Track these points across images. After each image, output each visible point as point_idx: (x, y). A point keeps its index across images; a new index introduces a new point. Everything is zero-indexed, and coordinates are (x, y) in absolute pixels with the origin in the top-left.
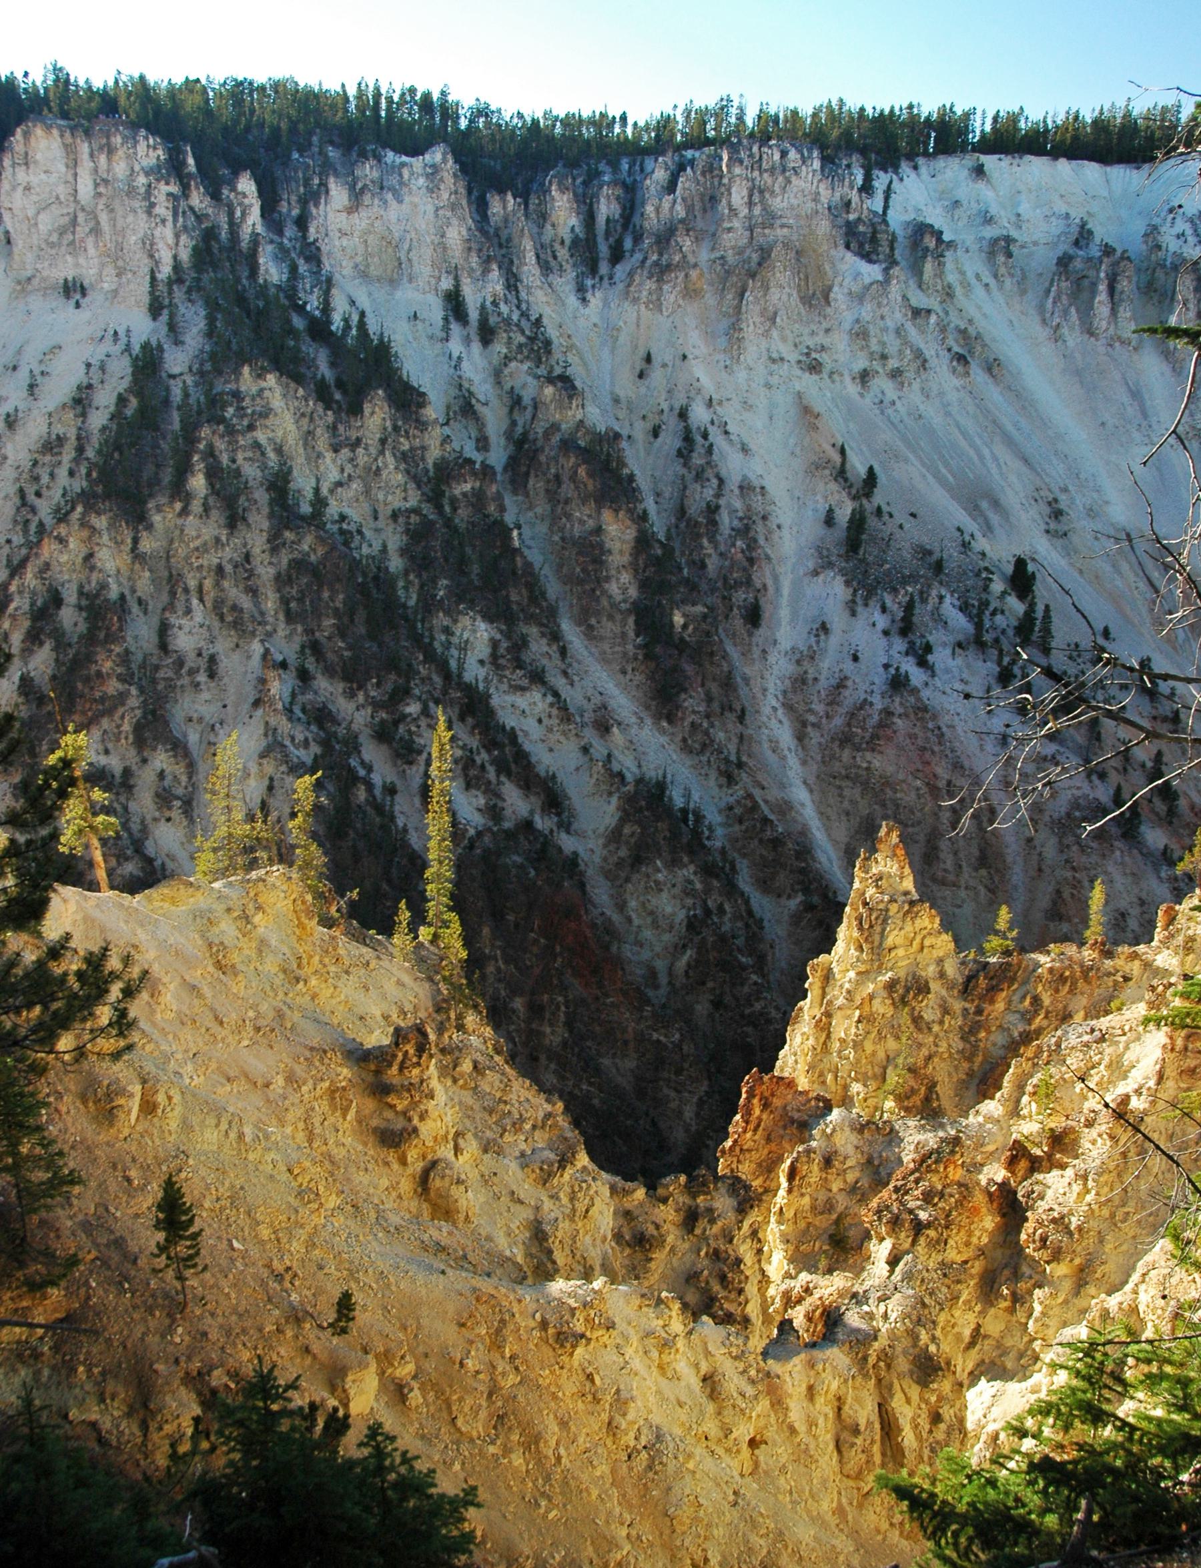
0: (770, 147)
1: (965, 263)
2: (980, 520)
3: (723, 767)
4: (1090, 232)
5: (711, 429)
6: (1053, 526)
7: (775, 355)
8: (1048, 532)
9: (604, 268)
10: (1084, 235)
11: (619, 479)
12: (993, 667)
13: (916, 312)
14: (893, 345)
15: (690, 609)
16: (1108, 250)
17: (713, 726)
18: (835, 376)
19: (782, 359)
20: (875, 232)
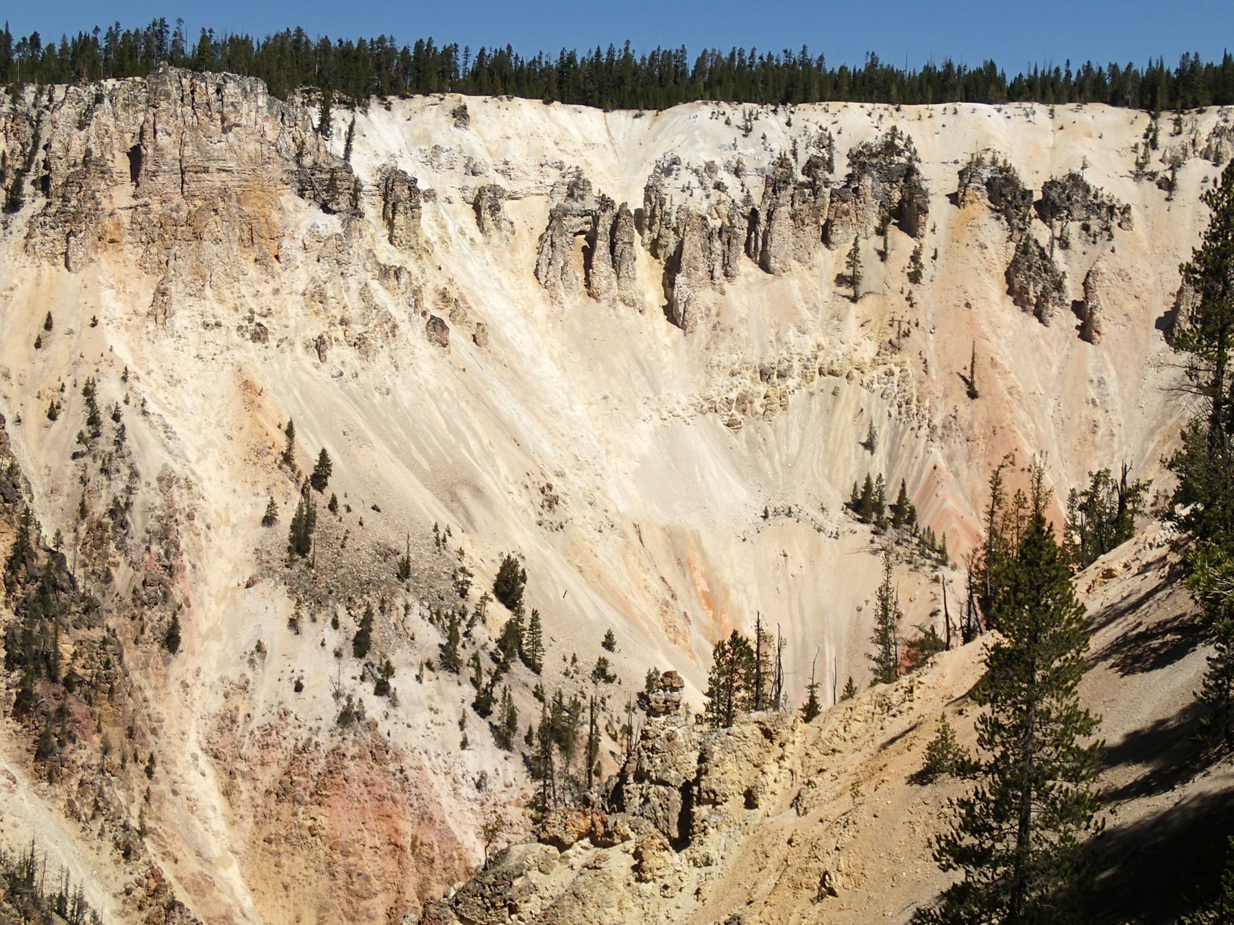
0: (204, 79)
1: (445, 219)
2: (460, 510)
3: (120, 836)
5: (124, 409)
6: (547, 516)
10: (576, 188)
12: (470, 693)
15: (83, 633)
16: (605, 203)
17: (109, 784)
18: (284, 345)
19: (218, 325)
20: (333, 180)
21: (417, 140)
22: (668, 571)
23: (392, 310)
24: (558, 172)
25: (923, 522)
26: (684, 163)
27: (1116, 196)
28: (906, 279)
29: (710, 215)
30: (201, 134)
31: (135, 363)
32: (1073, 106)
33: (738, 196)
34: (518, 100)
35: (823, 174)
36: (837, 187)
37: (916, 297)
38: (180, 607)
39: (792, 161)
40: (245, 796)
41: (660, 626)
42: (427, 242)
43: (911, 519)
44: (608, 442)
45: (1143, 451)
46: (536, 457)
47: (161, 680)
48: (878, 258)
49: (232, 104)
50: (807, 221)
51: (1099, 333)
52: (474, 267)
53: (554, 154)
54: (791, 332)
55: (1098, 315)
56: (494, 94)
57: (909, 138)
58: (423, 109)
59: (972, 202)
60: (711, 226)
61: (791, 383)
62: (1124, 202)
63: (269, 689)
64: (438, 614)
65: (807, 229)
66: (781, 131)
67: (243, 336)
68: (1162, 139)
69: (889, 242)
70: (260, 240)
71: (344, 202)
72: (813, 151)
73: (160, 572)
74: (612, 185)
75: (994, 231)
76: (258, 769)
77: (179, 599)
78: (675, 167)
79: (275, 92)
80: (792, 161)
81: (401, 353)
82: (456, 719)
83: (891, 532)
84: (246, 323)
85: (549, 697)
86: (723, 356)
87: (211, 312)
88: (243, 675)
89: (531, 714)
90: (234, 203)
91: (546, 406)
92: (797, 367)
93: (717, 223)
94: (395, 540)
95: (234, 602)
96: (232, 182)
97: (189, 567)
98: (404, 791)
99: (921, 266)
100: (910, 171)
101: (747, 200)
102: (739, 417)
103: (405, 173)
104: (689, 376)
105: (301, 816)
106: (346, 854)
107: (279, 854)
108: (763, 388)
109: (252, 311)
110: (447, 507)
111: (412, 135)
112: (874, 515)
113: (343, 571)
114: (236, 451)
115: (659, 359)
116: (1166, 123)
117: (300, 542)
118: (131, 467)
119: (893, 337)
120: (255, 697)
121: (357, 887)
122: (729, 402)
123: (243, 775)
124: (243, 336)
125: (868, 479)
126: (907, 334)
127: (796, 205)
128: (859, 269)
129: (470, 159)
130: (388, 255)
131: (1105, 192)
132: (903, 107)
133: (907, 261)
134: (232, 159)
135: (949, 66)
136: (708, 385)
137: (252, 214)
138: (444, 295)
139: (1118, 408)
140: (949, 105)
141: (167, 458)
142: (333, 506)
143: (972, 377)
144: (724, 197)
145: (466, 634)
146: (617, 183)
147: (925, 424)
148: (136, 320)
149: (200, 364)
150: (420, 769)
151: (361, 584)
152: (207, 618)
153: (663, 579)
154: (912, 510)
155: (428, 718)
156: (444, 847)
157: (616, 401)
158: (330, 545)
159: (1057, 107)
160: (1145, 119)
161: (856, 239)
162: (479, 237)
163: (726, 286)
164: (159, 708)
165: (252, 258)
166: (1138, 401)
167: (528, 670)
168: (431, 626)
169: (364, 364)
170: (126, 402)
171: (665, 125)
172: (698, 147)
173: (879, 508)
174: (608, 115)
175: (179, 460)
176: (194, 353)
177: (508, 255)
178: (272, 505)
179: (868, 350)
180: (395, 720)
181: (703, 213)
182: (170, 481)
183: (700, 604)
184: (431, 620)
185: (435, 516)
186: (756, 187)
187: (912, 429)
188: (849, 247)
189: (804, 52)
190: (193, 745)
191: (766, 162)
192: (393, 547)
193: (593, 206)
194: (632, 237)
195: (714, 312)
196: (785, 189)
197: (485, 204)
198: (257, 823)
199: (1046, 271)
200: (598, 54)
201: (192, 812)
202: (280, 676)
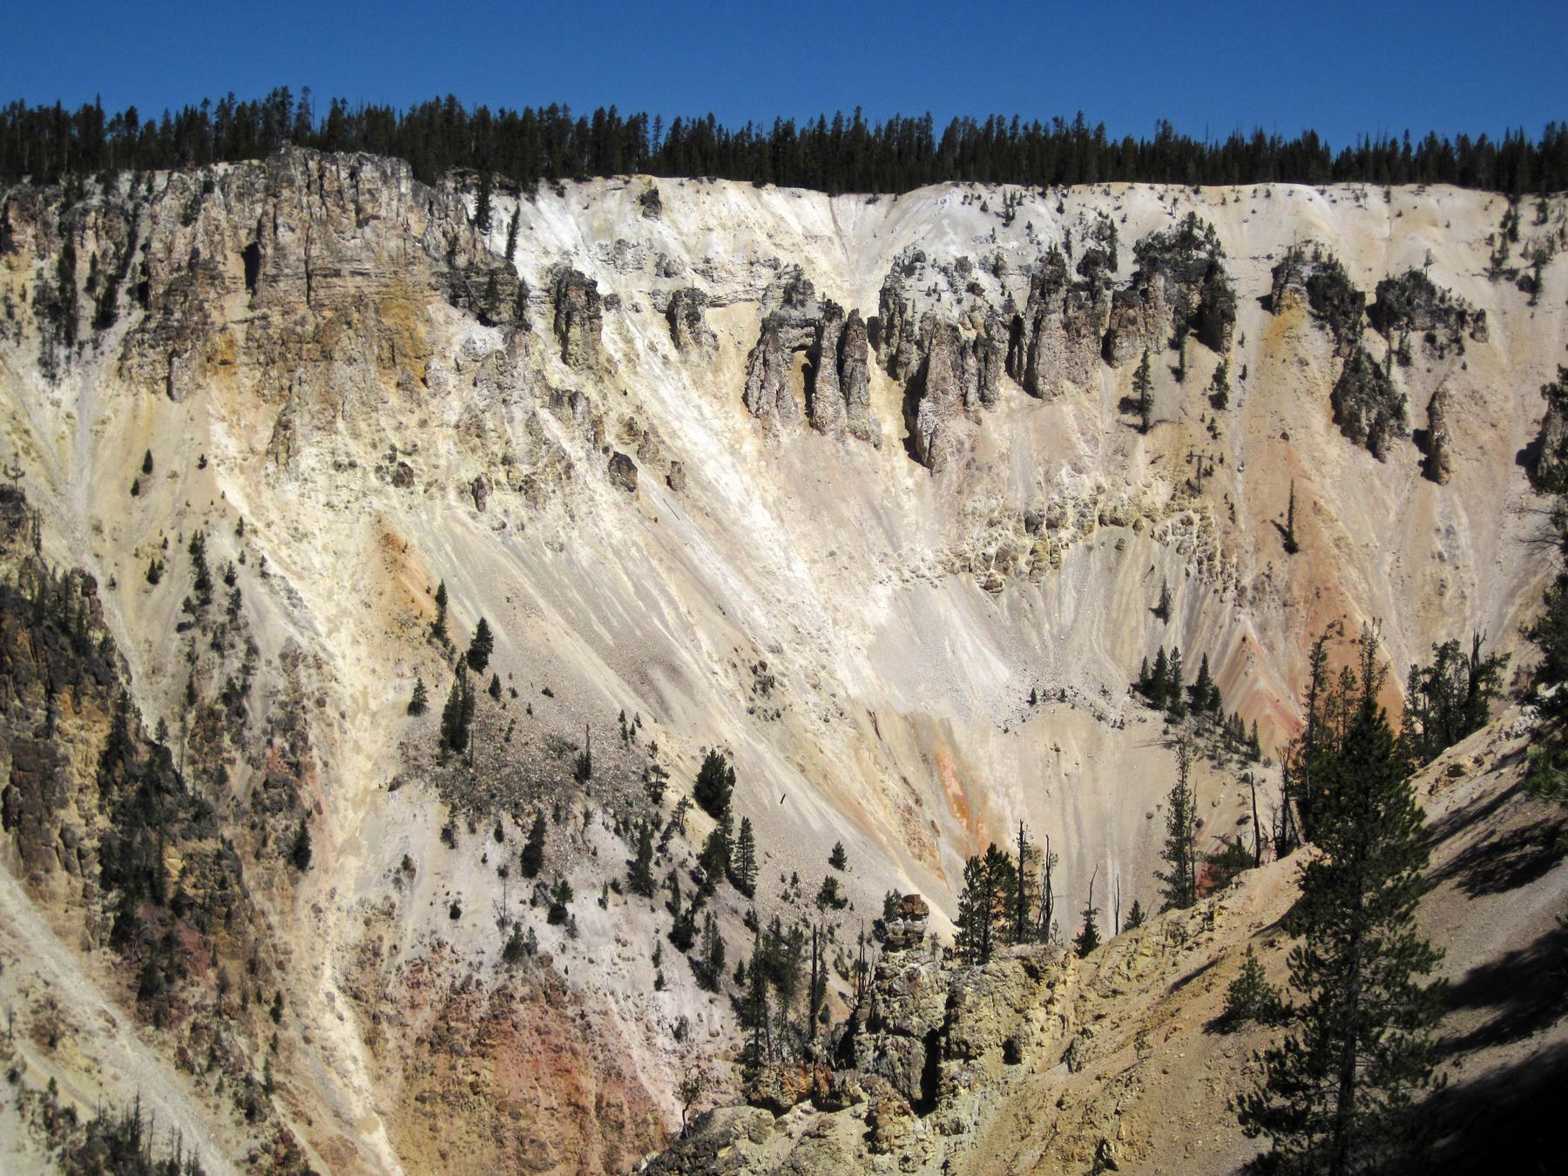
0: (334, 161)
1: (632, 330)
2: (652, 695)
3: (242, 1091)
4: (809, 285)
5: (238, 568)
6: (760, 702)
7: (345, 460)
8: (751, 712)
9: (85, 331)
10: (796, 289)
11: (82, 645)
12: (666, 921)
15: (193, 845)
16: (831, 310)
17: (228, 1028)
18: (433, 490)
19: (352, 465)
20: (492, 284)
21: (595, 233)
22: (911, 770)
23: (566, 445)
24: (771, 272)
25: (1229, 708)
26: (930, 260)
27: (1468, 300)
28: (1207, 403)
29: (963, 324)
31: (252, 513)
32: (1413, 187)
34: (722, 183)
36: (1121, 289)
37: (1220, 426)
38: (309, 814)
39: (1065, 256)
40: (391, 1045)
41: (901, 837)
42: (609, 360)
43: (1215, 702)
44: (836, 609)
45: (1501, 616)
46: (748, 631)
47: (289, 903)
48: (1173, 377)
49: (369, 191)
50: (1083, 331)
51: (1447, 471)
52: (667, 391)
53: (767, 249)
54: (1064, 472)
55: (1446, 448)
56: (692, 174)
57: (1211, 227)
58: (604, 194)
59: (1289, 307)
60: (964, 338)
61: (1065, 534)
62: (1477, 307)
63: (418, 915)
64: (626, 823)
65: (1084, 341)
67: (383, 479)
68: (1524, 229)
69: (1186, 357)
70: (405, 361)
71: (506, 312)
72: (1091, 244)
73: (283, 770)
74: (839, 288)
75: (1316, 344)
76: (408, 1012)
77: (308, 804)
78: (918, 264)
79: (423, 175)
80: (1065, 256)
81: (577, 499)
82: (648, 953)
83: (1189, 720)
84: (387, 463)
85: (764, 926)
86: (979, 501)
87: (344, 449)
88: (387, 898)
89: (741, 947)
90: (371, 314)
91: (758, 565)
93: (969, 335)
94: (571, 731)
95: (375, 808)
96: (369, 288)
97: (319, 765)
98: (585, 1040)
99: (1227, 387)
101: (1009, 306)
102: (999, 577)
103: (581, 275)
104: (937, 527)
105: (460, 1070)
106: (516, 1116)
107: (434, 1116)
108: (1028, 541)
109: (393, 448)
110: (636, 691)
111: (591, 227)
112: (1168, 703)
114: (375, 621)
115: (899, 506)
116: (1527, 210)
117: (455, 733)
118: (248, 641)
120: (403, 924)
121: (530, 1156)
122: (987, 558)
123: (389, 1019)
124: (383, 479)
125: (1161, 654)
126: (1209, 473)
127: (1070, 312)
128: (1150, 392)
129: (662, 256)
130: (560, 376)
132: (1204, 188)
133: (1208, 381)
134: (369, 259)
135: (1259, 137)
136: (960, 538)
137: (393, 327)
138: (630, 427)
139: (1471, 563)
140: (1261, 187)
141: (291, 630)
142: (495, 689)
143: (1290, 526)
144: (979, 302)
146: (846, 285)
147: (1231, 584)
148: (253, 460)
149: (330, 514)
150: (606, 1013)
151: (530, 787)
152: (342, 827)
153: (905, 779)
154: (1216, 692)
155: (614, 952)
156: (636, 1109)
157: (845, 559)
158: (492, 738)
159: (1395, 190)
160: (1502, 205)
161: (1145, 355)
162: (674, 355)
163: (983, 414)
164: (286, 938)
165: (393, 382)
166: (1495, 555)
167: (738, 893)
168: (617, 839)
169: (533, 513)
170: (242, 561)
171: (905, 212)
172: (947, 239)
173: (1174, 690)
174: (834, 200)
175: (306, 633)
176: (323, 500)
177: (709, 377)
178: (420, 689)
179: (1160, 493)
180: (573, 953)
181: (954, 322)
182: (296, 658)
183: (951, 812)
184: (617, 831)
185: (621, 702)
186: (1020, 289)
187: (1216, 591)
188: (1136, 363)
190: (328, 982)
191: (1032, 257)
192: (569, 740)
193: (815, 313)
194: (865, 352)
195: (967, 446)
196: (1056, 291)
197: (681, 312)
198: (407, 1078)
199: (1382, 393)
200: (822, 124)
201: (329, 1064)
202: (432, 898)
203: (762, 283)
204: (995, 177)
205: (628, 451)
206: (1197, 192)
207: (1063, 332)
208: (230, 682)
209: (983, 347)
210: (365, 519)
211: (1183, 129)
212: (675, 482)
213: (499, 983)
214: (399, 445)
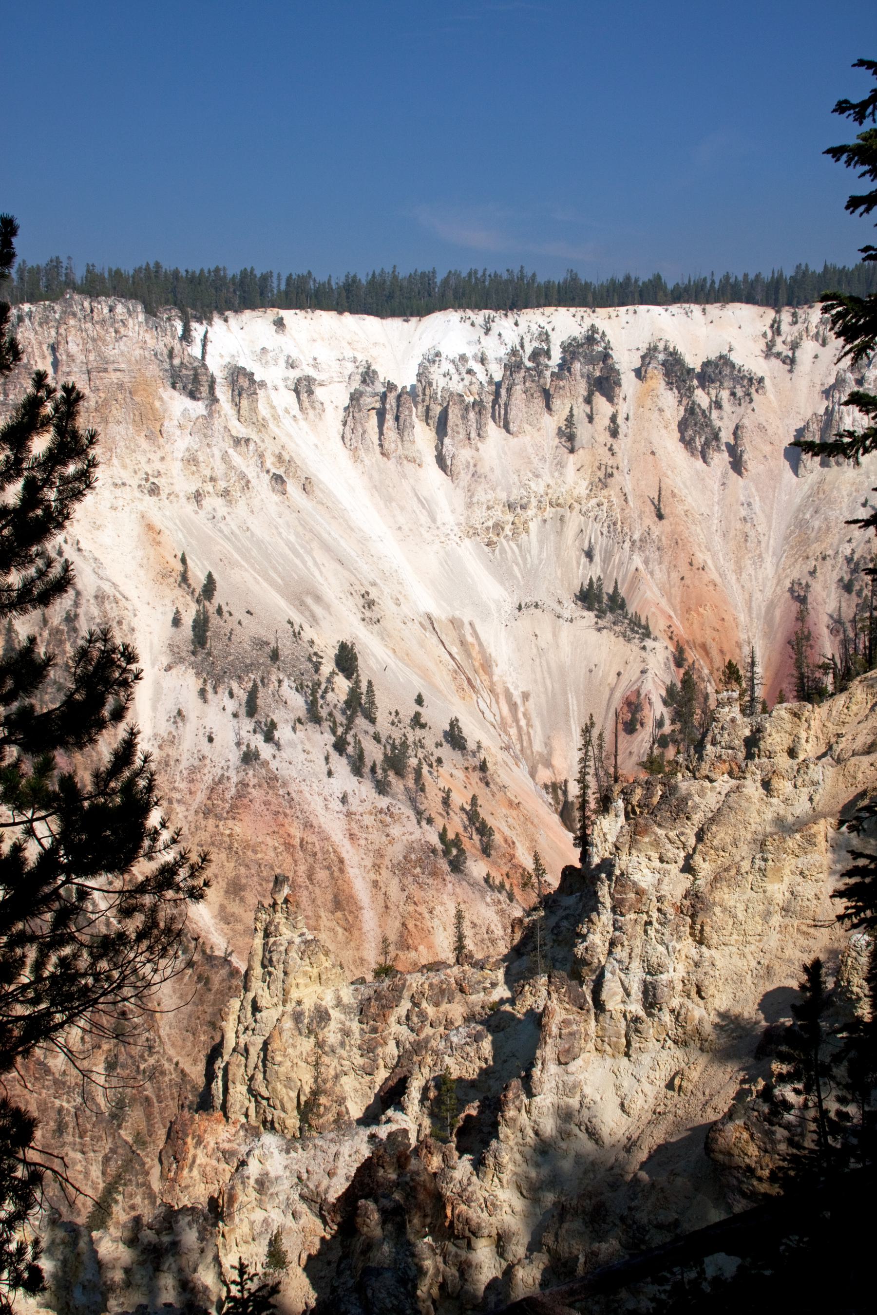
0: (99, 303)
4: (375, 372)
6: (368, 614)
8: (364, 620)
10: (368, 376)
13: (237, 442)
14: (220, 469)
16: (391, 386)
18: (172, 497)
19: (124, 484)
20: (196, 375)
25: (631, 609)
26: (444, 356)
28: (608, 434)
30: (100, 344)
33: (483, 378)
35: (543, 360)
37: (615, 447)
40: (180, 815)
43: (622, 606)
48: (587, 420)
55: (745, 457)
59: (652, 378)
61: (531, 512)
62: (760, 375)
64: (301, 684)
66: (514, 329)
68: (785, 327)
72: (536, 344)
75: (669, 399)
79: (150, 311)
83: (609, 616)
84: (144, 482)
85: (383, 740)
89: (374, 753)
92: (534, 502)
98: (291, 807)
100: (606, 356)
103: (244, 369)
105: (221, 827)
106: (255, 852)
108: (510, 517)
112: (596, 606)
113: (232, 658)
116: (786, 316)
119: (602, 476)
121: (265, 874)
123: (179, 801)
125: (591, 579)
126: (611, 475)
127: (527, 384)
130: (239, 430)
131: (746, 368)
132: (597, 310)
133: (607, 422)
135: (628, 278)
138: (280, 458)
140: (631, 308)
142: (219, 611)
145: (323, 697)
147: (627, 538)
154: (623, 599)
159: (708, 307)
160: (771, 314)
161: (571, 409)
163: (479, 445)
167: (367, 722)
169: (230, 510)
179: (582, 489)
182: (103, 598)
184: (297, 690)
188: (566, 412)
189: (521, 271)
191: (502, 352)
194: (411, 411)
196: (519, 372)
203: (347, 373)
204: (478, 306)
205: (280, 472)
206: (594, 312)
207: (524, 396)
208: (67, 613)
209: (478, 405)
210: (134, 516)
211: (585, 277)
212: (308, 487)
213: (240, 779)
214: (150, 472)
